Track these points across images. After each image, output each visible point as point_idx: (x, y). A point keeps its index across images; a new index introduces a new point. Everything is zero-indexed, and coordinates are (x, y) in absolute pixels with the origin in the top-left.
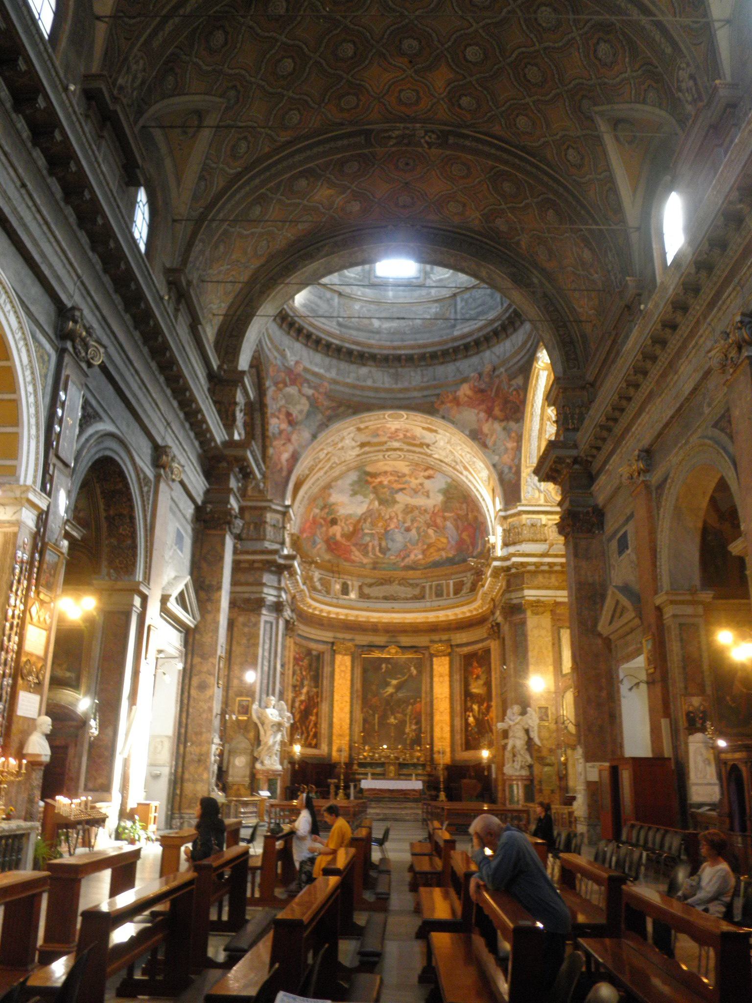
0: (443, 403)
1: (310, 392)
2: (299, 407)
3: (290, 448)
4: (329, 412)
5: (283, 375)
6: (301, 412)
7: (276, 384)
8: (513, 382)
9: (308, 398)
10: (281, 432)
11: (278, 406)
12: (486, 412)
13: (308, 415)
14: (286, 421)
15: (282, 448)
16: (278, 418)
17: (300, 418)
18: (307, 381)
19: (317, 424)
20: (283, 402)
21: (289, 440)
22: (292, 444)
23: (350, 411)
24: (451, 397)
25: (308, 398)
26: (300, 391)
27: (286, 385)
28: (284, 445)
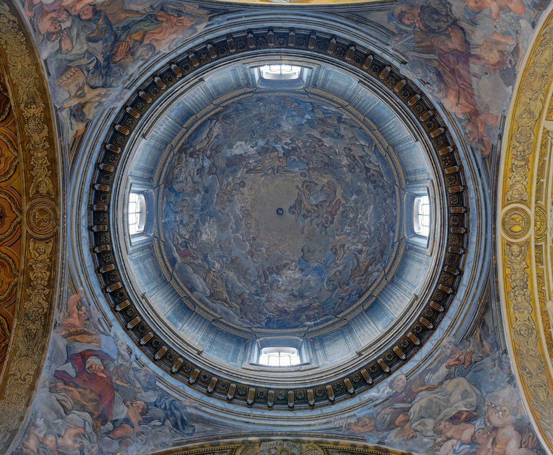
0: (481, 141)
1: (443, 371)
2: (456, 397)
3: (510, 431)
4: (487, 347)
5: (388, 410)
6: (465, 395)
7: (391, 426)
8: (392, 26)
9: (449, 377)
10: (473, 442)
11: (431, 433)
12: (466, 63)
13: (476, 383)
14: (463, 426)
15: (498, 449)
16: (449, 439)
17: (473, 399)
18: (426, 372)
19: (496, 368)
20: (430, 423)
21: (496, 429)
22: (503, 427)
23: (494, 305)
24: (469, 128)
25: (449, 377)
26: (430, 389)
27: (406, 411)
28: (494, 443)
